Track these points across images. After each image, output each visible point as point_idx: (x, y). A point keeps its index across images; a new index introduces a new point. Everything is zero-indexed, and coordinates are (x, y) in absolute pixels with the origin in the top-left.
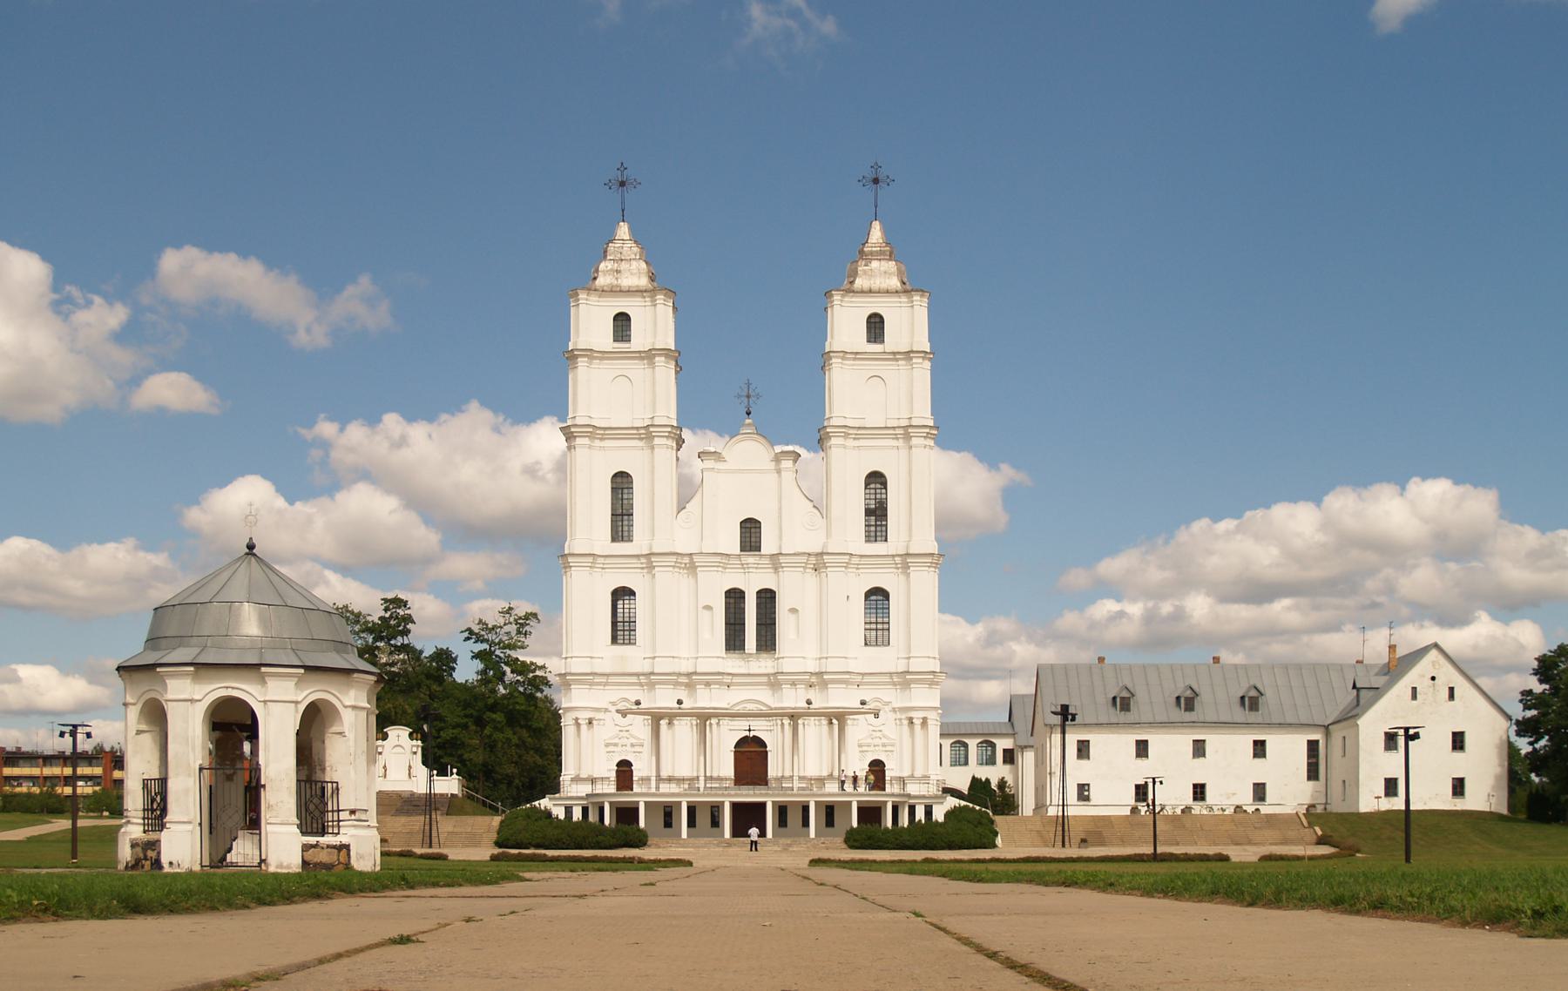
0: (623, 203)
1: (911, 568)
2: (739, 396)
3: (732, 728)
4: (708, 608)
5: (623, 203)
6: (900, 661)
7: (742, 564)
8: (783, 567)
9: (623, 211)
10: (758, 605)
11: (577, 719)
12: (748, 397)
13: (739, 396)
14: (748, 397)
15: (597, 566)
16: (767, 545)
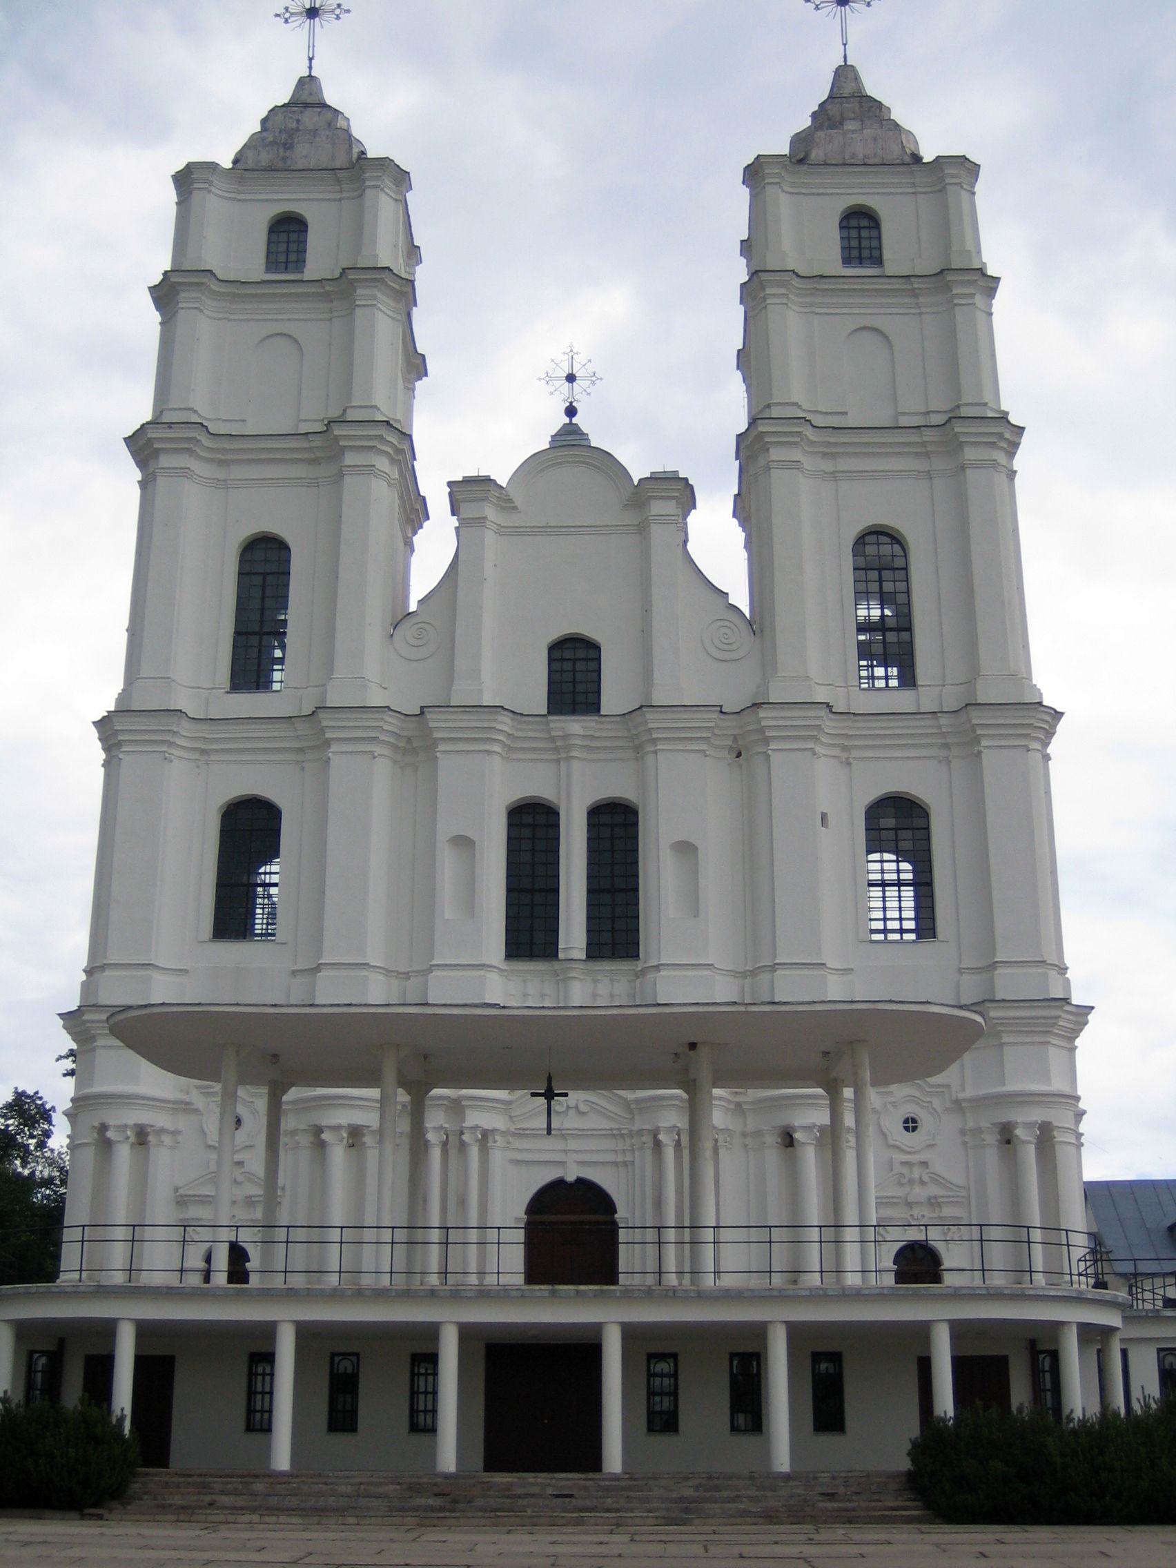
0: (311, 46)
1: (984, 743)
2: (549, 379)
3: (520, 1157)
4: (464, 843)
5: (311, 46)
6: (965, 977)
7: (552, 739)
8: (654, 741)
9: (311, 59)
10: (592, 851)
11: (103, 1128)
12: (571, 378)
13: (549, 379)
14: (571, 378)
15: (180, 742)
16: (615, 697)
